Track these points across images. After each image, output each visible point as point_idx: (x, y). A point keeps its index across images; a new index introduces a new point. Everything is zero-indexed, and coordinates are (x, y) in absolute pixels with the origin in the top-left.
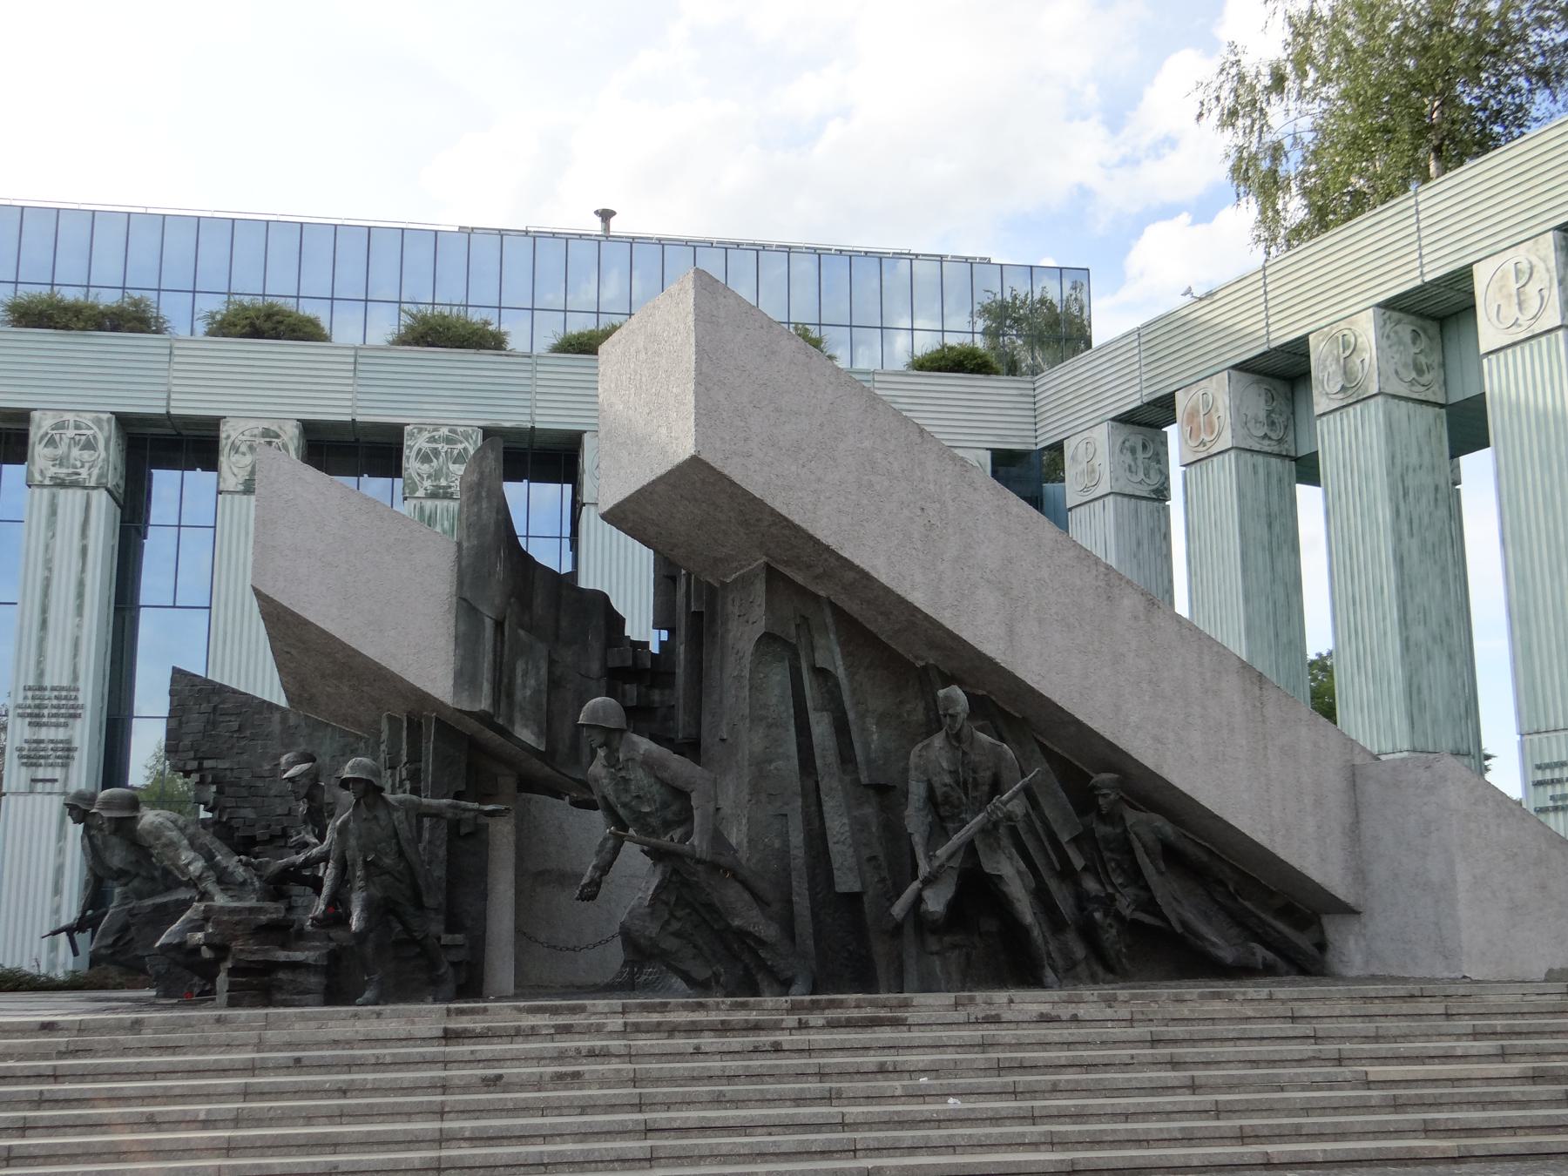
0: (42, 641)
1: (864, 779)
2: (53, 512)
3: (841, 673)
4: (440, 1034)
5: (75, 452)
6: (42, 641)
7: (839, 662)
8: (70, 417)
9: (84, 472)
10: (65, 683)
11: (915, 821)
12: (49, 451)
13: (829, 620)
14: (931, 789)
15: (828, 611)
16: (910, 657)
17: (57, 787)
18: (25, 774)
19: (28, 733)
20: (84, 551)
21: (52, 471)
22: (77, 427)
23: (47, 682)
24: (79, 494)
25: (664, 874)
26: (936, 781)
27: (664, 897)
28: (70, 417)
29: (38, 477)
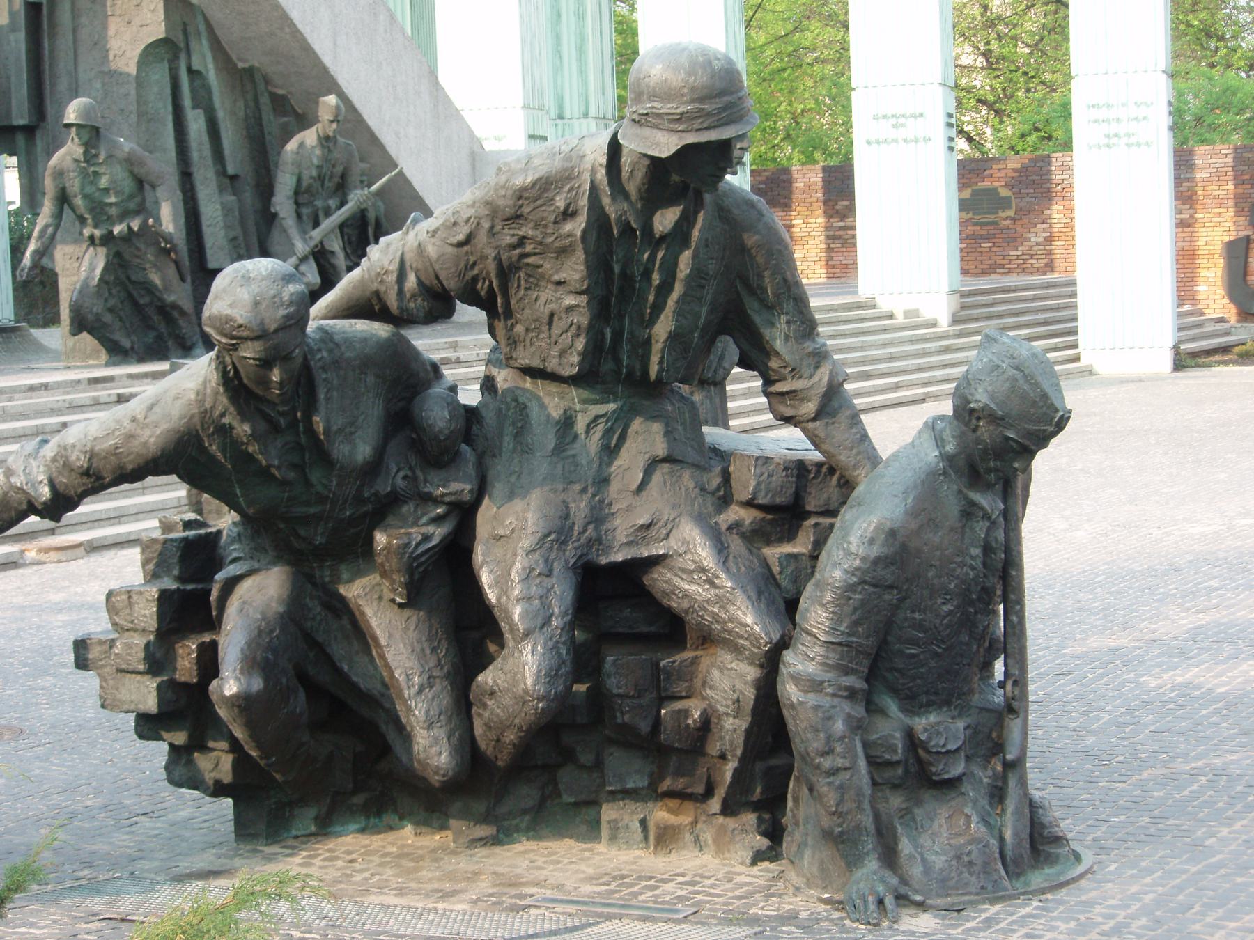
1: (231, 170)
3: (212, 76)
4: (115, 399)
7: (211, 66)
11: (282, 203)
13: (202, 27)
14: (299, 181)
15: (200, 18)
16: (234, 58)
25: (107, 256)
26: (306, 175)
27: (107, 277)
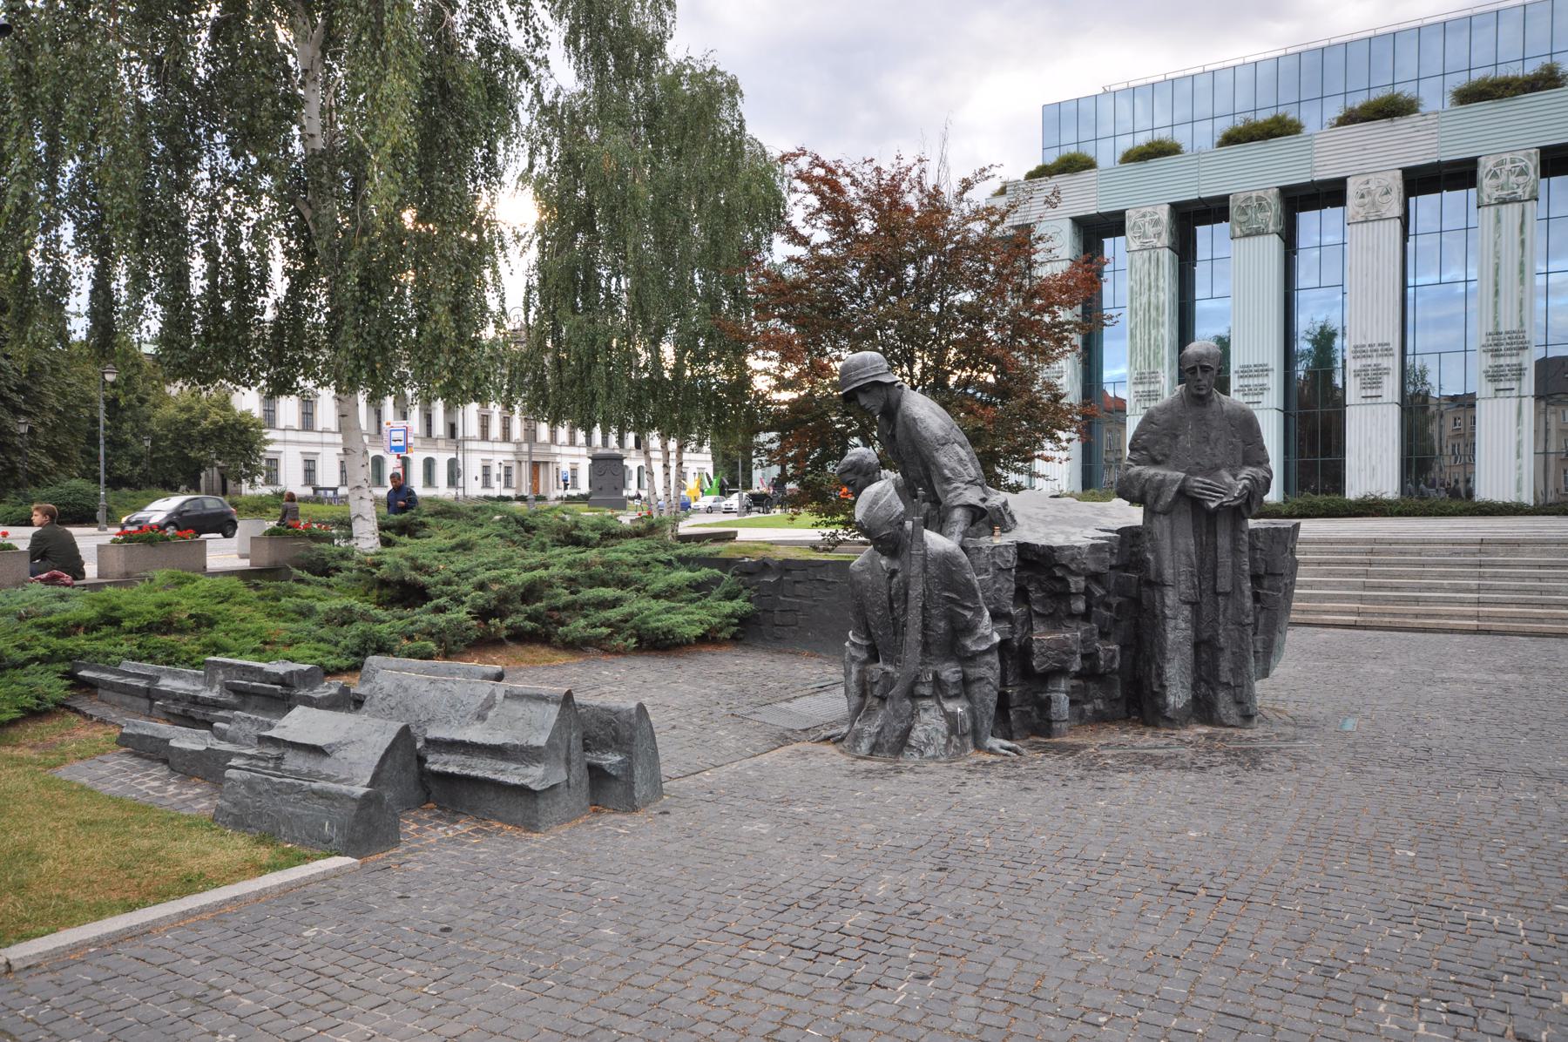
0: (1496, 304)
2: (1498, 221)
5: (1512, 178)
6: (1496, 304)
8: (1504, 156)
9: (1520, 192)
10: (1515, 328)
12: (1494, 182)
17: (1514, 393)
18: (1491, 387)
19: (1491, 362)
20: (1523, 242)
21: (1496, 194)
22: (1513, 162)
23: (1502, 329)
24: (1516, 205)
28: (1508, 157)
29: (1486, 200)
